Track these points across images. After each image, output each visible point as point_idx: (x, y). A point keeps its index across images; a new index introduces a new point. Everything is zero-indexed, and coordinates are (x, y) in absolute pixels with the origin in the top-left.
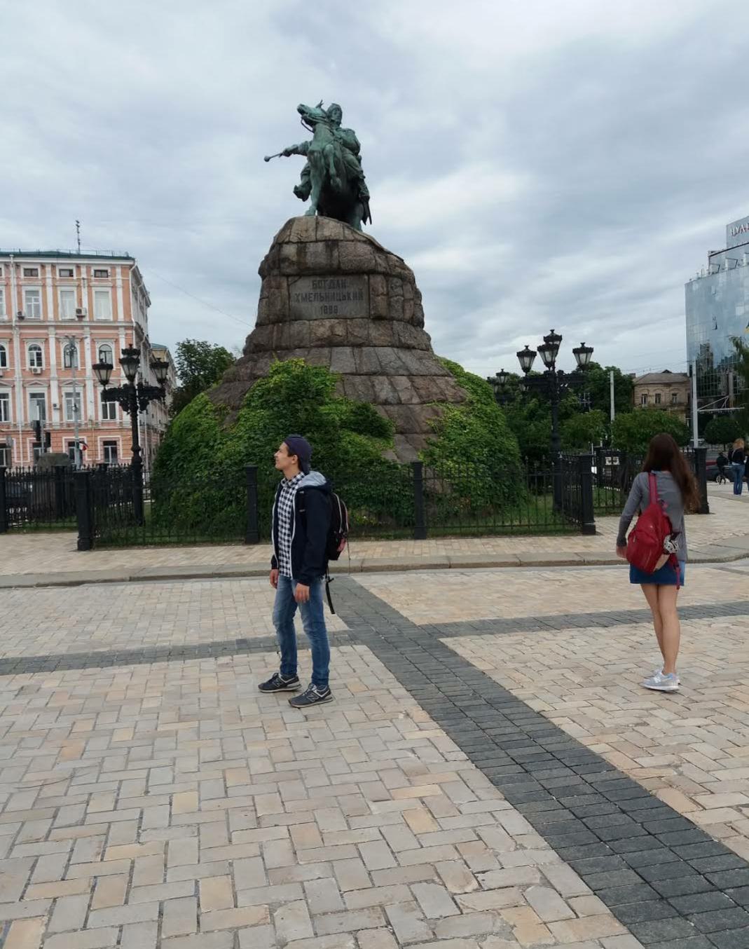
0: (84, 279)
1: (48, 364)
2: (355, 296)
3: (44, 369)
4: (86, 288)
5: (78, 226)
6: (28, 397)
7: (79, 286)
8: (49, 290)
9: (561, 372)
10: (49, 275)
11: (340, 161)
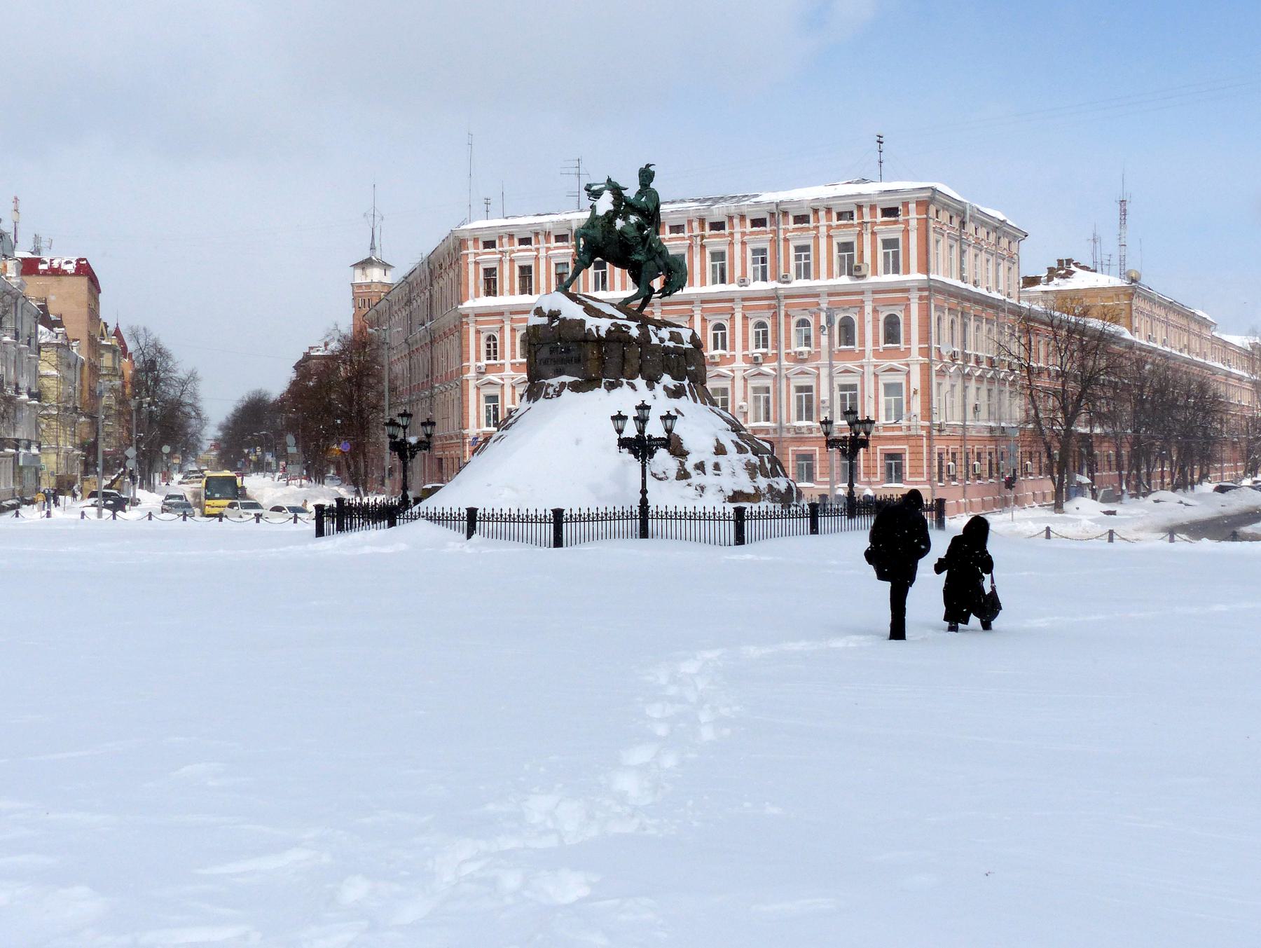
0: (865, 223)
1: (818, 344)
2: (576, 362)
3: (813, 352)
4: (870, 235)
5: (882, 143)
6: (793, 390)
7: (860, 235)
8: (823, 242)
9: (650, 436)
10: (823, 222)
11: (595, 238)
